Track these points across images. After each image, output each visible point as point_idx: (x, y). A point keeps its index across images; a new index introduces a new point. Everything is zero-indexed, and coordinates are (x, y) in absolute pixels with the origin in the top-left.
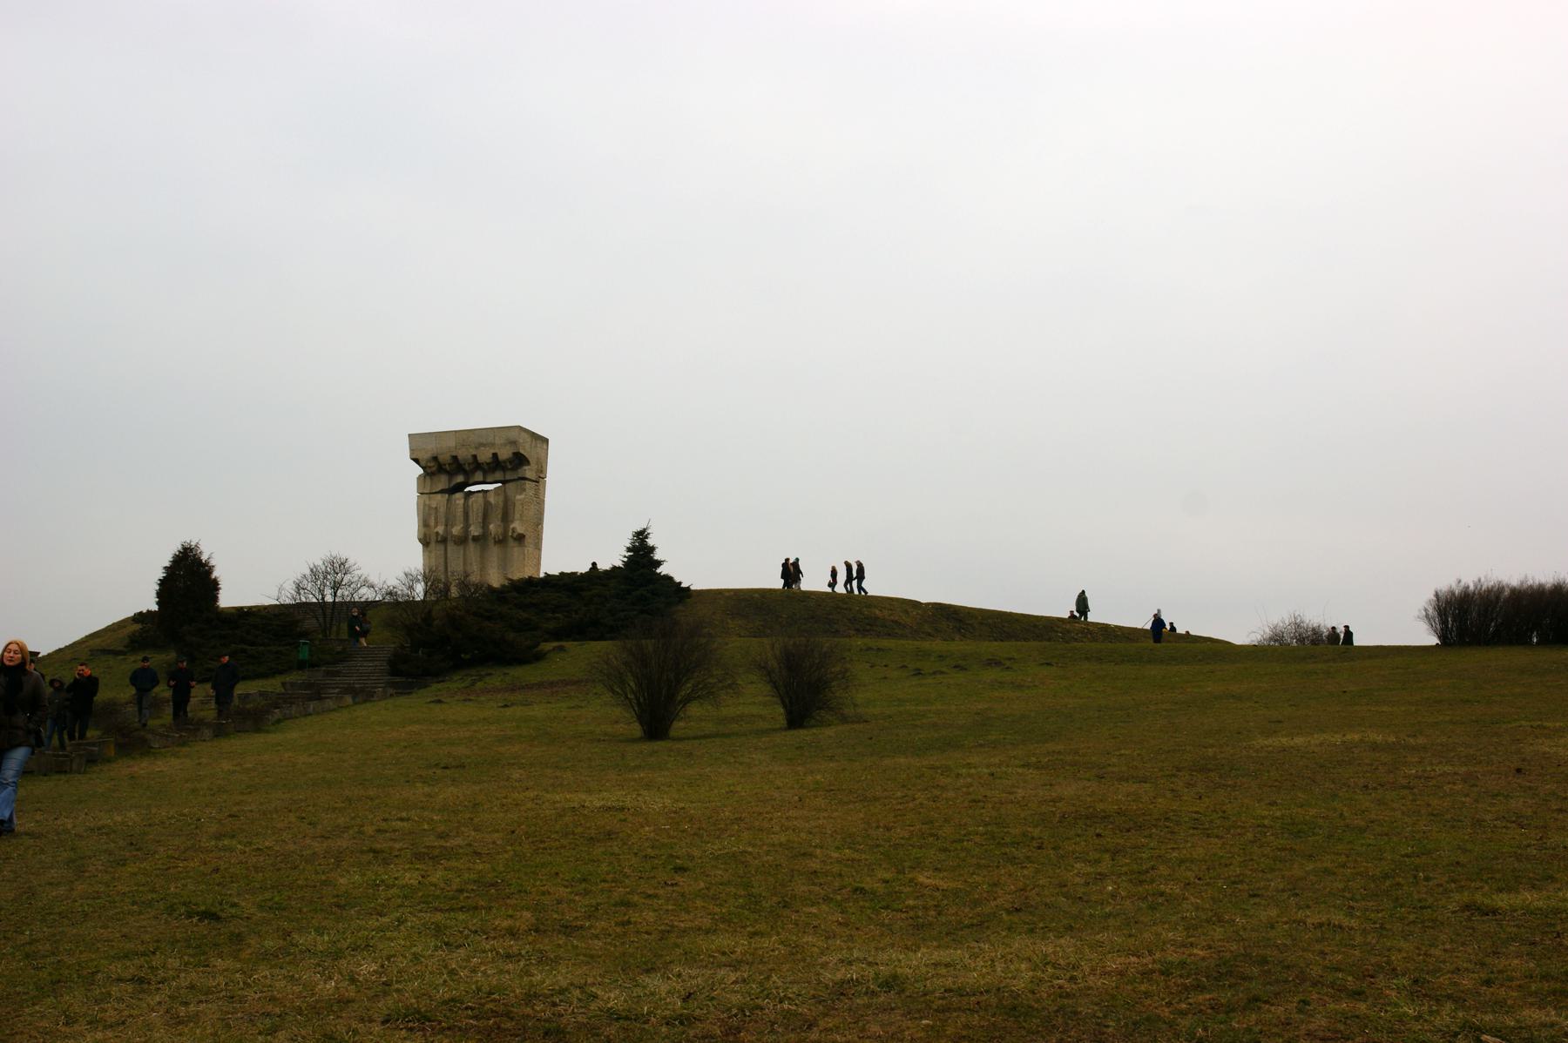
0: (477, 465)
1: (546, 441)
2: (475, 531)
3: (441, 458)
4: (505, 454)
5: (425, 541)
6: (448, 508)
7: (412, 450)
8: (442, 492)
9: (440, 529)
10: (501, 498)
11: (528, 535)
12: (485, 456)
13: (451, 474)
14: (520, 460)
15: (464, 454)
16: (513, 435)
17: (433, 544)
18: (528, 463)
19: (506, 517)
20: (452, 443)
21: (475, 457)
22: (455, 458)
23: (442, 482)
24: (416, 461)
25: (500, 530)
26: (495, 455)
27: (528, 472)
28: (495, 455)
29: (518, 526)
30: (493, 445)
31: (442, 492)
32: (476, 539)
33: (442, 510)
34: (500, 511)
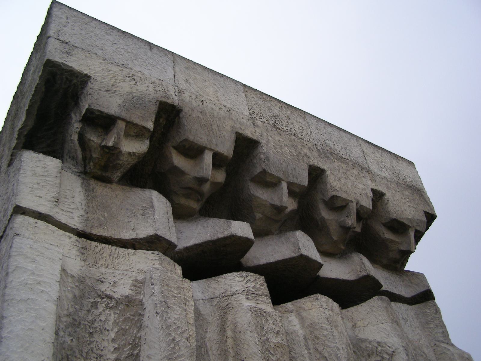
21: (316, 174)
23: (152, 214)
31: (154, 243)
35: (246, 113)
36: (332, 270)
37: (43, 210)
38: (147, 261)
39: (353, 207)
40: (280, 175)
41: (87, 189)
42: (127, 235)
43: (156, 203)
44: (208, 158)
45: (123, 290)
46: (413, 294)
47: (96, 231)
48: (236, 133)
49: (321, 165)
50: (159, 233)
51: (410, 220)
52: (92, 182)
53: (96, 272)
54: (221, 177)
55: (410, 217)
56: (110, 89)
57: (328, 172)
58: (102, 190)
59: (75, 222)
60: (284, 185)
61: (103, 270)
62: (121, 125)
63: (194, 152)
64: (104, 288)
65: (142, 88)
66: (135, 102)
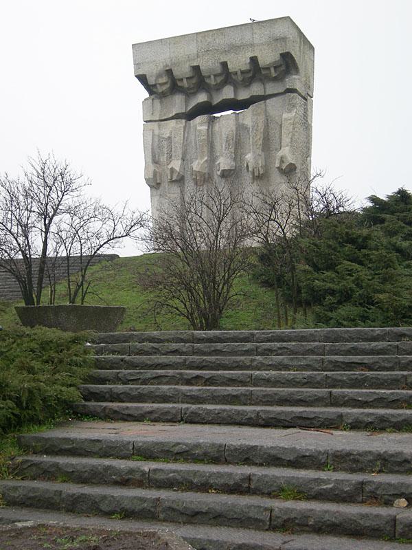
0: (226, 77)
1: (312, 48)
2: (224, 163)
4: (268, 57)
5: (155, 184)
6: (185, 139)
7: (137, 65)
9: (176, 164)
10: (262, 119)
11: (298, 166)
13: (189, 93)
14: (288, 64)
15: (208, 64)
16: (280, 30)
17: (165, 185)
18: (297, 70)
19: (267, 145)
20: (192, 49)
21: (224, 65)
22: (196, 69)
23: (178, 104)
24: (142, 79)
25: (261, 162)
26: (254, 60)
27: (295, 81)
28: (254, 60)
29: (286, 153)
30: (252, 45)
32: (225, 175)
33: (178, 139)
34: (260, 135)
36: (244, 95)
37: (149, 119)
39: (239, 73)
41: (161, 102)
42: (171, 115)
43: (177, 101)
44: (185, 81)
45: (168, 135)
47: (163, 118)
50: (178, 112)
52: (163, 99)
54: (194, 81)
56: (151, 71)
59: (157, 119)
60: (212, 77)
62: (158, 85)
63: (182, 80)
66: (159, 76)
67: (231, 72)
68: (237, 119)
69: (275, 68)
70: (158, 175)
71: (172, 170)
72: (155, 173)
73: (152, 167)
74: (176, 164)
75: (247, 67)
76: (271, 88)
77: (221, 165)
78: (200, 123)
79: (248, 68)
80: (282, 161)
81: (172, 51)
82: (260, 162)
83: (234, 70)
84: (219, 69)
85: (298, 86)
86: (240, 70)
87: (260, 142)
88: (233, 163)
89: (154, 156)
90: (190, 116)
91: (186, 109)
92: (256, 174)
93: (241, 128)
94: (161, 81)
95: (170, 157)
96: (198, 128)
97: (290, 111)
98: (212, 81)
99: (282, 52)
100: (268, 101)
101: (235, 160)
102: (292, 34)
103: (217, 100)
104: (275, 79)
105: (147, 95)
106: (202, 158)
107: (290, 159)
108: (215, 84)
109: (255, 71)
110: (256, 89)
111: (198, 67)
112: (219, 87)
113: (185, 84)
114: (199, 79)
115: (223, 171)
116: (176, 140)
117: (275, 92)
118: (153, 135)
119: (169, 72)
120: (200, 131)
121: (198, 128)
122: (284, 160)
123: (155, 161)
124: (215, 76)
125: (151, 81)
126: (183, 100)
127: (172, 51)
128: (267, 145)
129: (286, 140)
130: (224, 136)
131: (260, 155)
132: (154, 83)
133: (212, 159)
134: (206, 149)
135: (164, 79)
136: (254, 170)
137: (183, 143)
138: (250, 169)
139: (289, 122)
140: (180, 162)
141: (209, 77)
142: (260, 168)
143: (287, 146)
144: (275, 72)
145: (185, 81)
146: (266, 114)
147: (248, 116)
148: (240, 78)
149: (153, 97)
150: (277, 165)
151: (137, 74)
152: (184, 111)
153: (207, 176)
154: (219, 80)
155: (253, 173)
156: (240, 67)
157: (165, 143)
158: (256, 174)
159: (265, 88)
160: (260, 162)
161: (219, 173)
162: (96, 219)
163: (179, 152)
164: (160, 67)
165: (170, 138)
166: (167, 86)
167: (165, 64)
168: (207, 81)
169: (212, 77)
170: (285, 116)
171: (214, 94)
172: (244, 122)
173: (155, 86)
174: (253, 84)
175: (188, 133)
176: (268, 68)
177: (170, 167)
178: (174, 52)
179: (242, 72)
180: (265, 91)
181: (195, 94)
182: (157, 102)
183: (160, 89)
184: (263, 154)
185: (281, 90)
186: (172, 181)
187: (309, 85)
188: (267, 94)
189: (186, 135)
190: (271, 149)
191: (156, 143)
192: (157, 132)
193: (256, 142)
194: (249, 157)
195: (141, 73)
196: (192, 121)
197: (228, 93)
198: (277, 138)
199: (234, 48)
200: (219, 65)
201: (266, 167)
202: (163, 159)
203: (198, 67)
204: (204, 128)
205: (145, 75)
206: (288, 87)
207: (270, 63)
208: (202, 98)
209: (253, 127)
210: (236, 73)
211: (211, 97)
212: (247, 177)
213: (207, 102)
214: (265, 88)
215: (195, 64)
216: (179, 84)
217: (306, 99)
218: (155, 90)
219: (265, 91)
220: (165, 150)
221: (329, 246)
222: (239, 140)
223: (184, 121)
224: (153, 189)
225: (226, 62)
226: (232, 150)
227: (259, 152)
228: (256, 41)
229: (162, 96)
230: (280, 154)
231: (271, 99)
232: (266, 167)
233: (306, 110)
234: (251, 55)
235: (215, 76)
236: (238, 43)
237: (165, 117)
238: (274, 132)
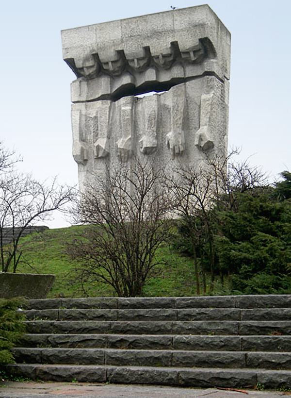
0: (149, 60)
1: (228, 34)
2: (147, 140)
3: (103, 57)
4: (187, 42)
5: (82, 161)
6: (111, 118)
8: (103, 98)
9: (102, 142)
10: (182, 100)
11: (216, 144)
12: (160, 47)
13: (114, 76)
14: (206, 48)
15: (132, 49)
17: (92, 161)
18: (214, 54)
19: (187, 124)
20: (116, 34)
21: (147, 49)
22: (121, 53)
23: (104, 86)
24: (70, 62)
25: (181, 140)
26: (174, 45)
27: (213, 65)
28: (174, 45)
30: (173, 31)
31: (103, 98)
32: (148, 152)
33: (104, 119)
34: (180, 115)
35: (120, 37)
36: (165, 78)
37: (76, 100)
38: (99, 103)
39: (161, 57)
40: (132, 58)
42: (97, 96)
44: (110, 64)
45: (94, 115)
46: (203, 73)
47: (90, 99)
48: (116, 51)
49: (148, 45)
50: (103, 93)
51: (188, 49)
52: (90, 81)
53: (89, 112)
54: (119, 64)
55: (187, 48)
56: (79, 55)
57: (150, 47)
58: (92, 82)
59: (84, 100)
60: (136, 61)
61: (90, 110)
62: (85, 69)
63: (107, 63)
64: (90, 116)
65: (86, 52)
66: (86, 59)
67: (154, 56)
68: (158, 100)
69: (194, 52)
70: (85, 152)
71: (98, 148)
72: (82, 150)
73: (79, 145)
74: (102, 142)
75: (168, 52)
76: (190, 71)
77: (144, 143)
78: (124, 104)
79: (169, 52)
80: (201, 139)
81: (98, 36)
82: (180, 140)
83: (156, 54)
84: (142, 54)
85: (216, 69)
86: (162, 54)
87: (180, 122)
88: (155, 141)
89: (81, 135)
90: (115, 97)
91: (111, 91)
92: (177, 151)
93: (162, 108)
94: (88, 64)
95: (96, 136)
96: (123, 108)
97: (208, 92)
98: (135, 65)
99: (201, 37)
100: (188, 83)
101: (157, 138)
102: (210, 21)
103: (140, 82)
104: (194, 63)
105: (74, 77)
106: (126, 136)
107: (208, 137)
108: (138, 67)
109: (176, 56)
110: (177, 72)
111: (122, 51)
112: (142, 70)
113: (110, 67)
114: (123, 63)
115: (146, 148)
116: (102, 119)
117: (194, 75)
118: (81, 115)
119: (96, 56)
120: (124, 111)
121: (123, 108)
122: (203, 138)
123: (83, 139)
124: (138, 59)
125: (79, 64)
126: (109, 82)
127: (98, 36)
128: (187, 124)
129: (204, 119)
130: (147, 116)
131: (180, 134)
132: (81, 66)
133: (136, 137)
134: (129, 128)
135: (90, 63)
136: (174, 147)
137: (109, 122)
138: (171, 147)
139: (208, 102)
140: (105, 140)
141: (133, 60)
142: (180, 146)
143: (206, 125)
144: (194, 55)
145: (110, 64)
146: (186, 95)
147: (169, 98)
148: (162, 61)
149: (80, 79)
150: (196, 143)
151: (66, 58)
152: (109, 92)
153: (130, 153)
154: (142, 63)
155: (174, 150)
156: (161, 52)
157: (92, 122)
158: (177, 151)
159: (184, 71)
160: (180, 140)
161: (142, 150)
162: (27, 193)
163: (105, 131)
164: (87, 52)
165: (96, 117)
166: (94, 69)
167: (91, 48)
168: (131, 64)
169: (136, 61)
170: (204, 97)
171: (137, 76)
172: (165, 103)
173: (82, 69)
174: (174, 68)
175: (113, 113)
176: (187, 53)
177: (96, 144)
178: (100, 37)
179: (164, 56)
180: (185, 74)
181: (119, 76)
182: (84, 85)
183: (87, 72)
184: (183, 132)
185: (200, 73)
186: (98, 158)
187: (225, 69)
188: (187, 76)
189: (111, 115)
190: (191, 128)
191: (84, 122)
192: (84, 112)
193: (176, 121)
194: (170, 135)
195: (69, 57)
196: (116, 102)
197: (150, 76)
198: (196, 118)
199: (156, 34)
200: (141, 49)
201: (186, 145)
202: (90, 137)
203: (122, 51)
204: (129, 108)
205: (73, 59)
206: (206, 70)
207: (189, 48)
208: (126, 80)
209: (174, 107)
210: (158, 57)
211: (134, 79)
212: (168, 154)
213: (155, 81)
214: (184, 71)
215: (120, 49)
216: (105, 67)
217: (223, 81)
218: (82, 73)
219: (185, 74)
220: (92, 129)
221: (245, 219)
222: (161, 119)
223: (109, 102)
224: (80, 165)
225: (149, 47)
226: (154, 129)
227: (179, 130)
228: (177, 27)
229: (89, 78)
230: (199, 132)
231: (191, 82)
232: (186, 145)
233: (223, 92)
234: (171, 40)
235: (138, 59)
236: (160, 29)
237: (92, 98)
238: (193, 112)
